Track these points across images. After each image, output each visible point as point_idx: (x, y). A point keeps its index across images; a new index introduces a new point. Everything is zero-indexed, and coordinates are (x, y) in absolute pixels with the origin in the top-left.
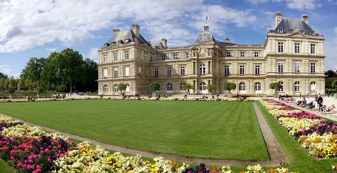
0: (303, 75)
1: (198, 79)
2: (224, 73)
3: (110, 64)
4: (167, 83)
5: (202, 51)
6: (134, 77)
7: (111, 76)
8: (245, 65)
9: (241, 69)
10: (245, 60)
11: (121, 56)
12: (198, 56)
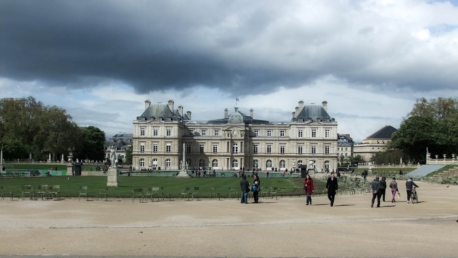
0: (318, 155)
1: (231, 156)
3: (149, 138)
4: (199, 159)
5: (235, 133)
6: (176, 153)
8: (271, 145)
9: (268, 148)
10: (272, 140)
11: (162, 132)
12: (231, 136)
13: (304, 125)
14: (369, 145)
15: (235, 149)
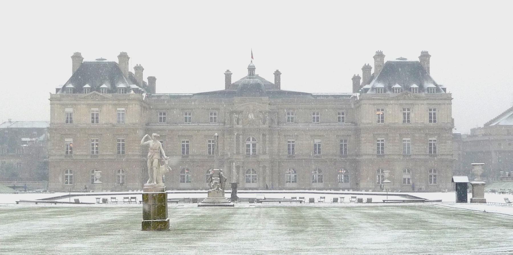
2: (287, 153)
5: (251, 116)
7: (85, 153)
14: (492, 138)
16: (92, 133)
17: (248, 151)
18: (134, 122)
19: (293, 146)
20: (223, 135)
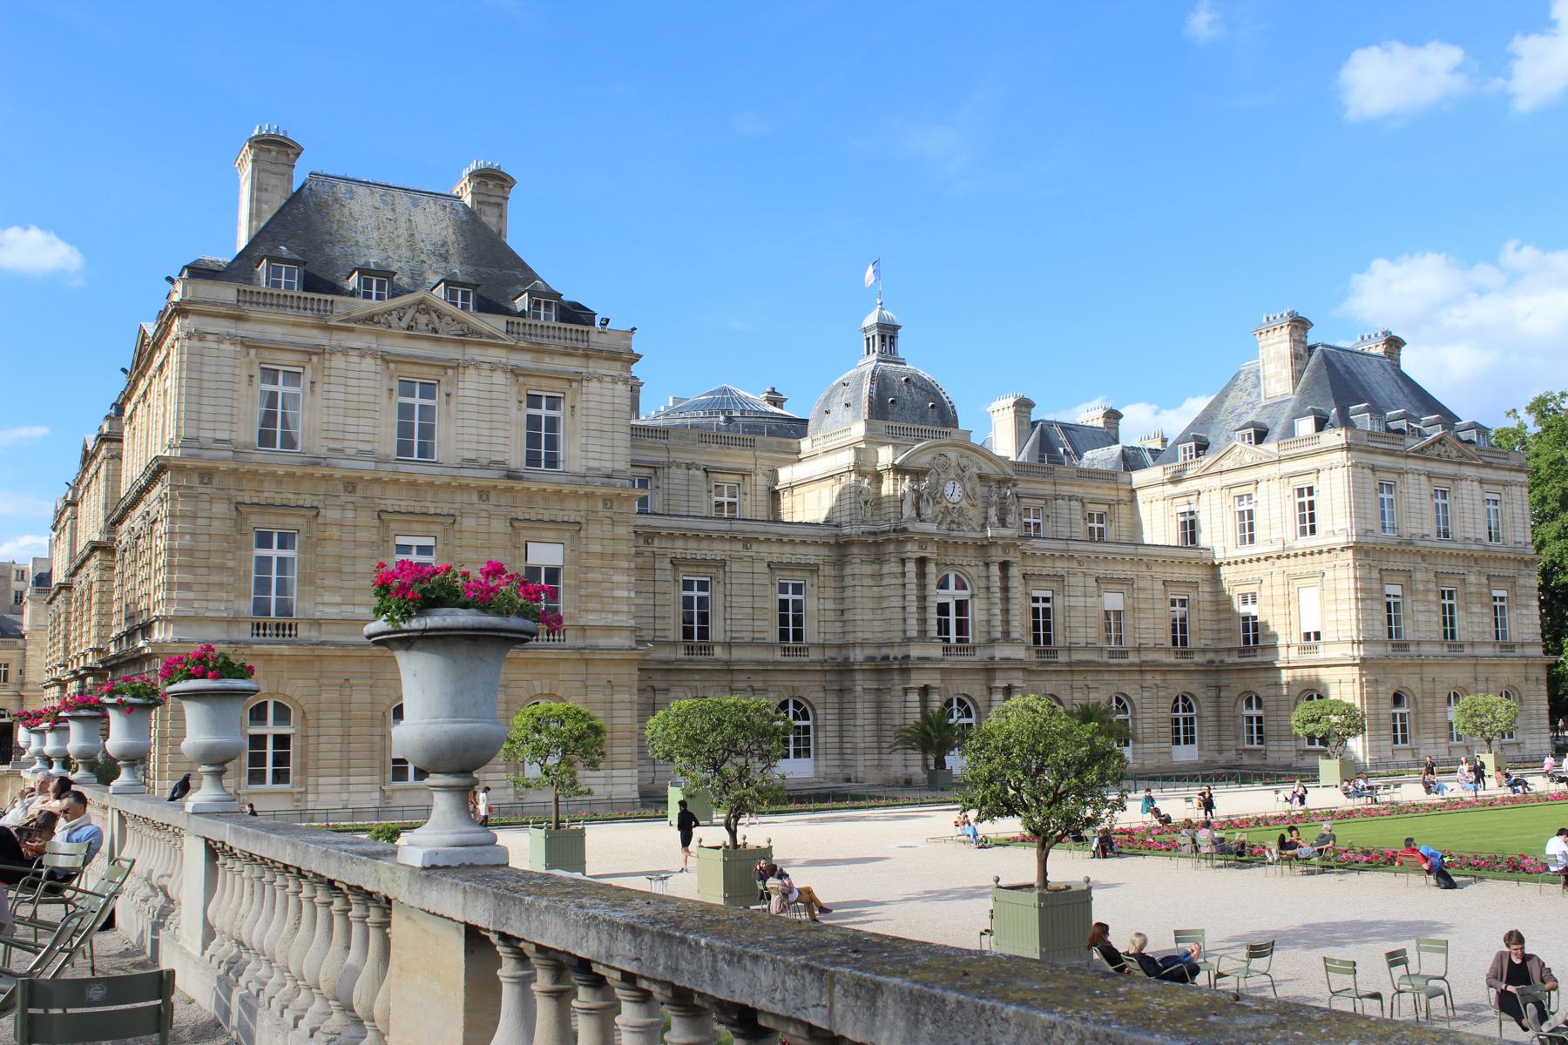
5: (954, 492)
6: (622, 640)
13: (1408, 457)
15: (952, 618)
16: (404, 506)
17: (943, 628)
18: (607, 466)
19: (1047, 611)
20: (841, 562)
